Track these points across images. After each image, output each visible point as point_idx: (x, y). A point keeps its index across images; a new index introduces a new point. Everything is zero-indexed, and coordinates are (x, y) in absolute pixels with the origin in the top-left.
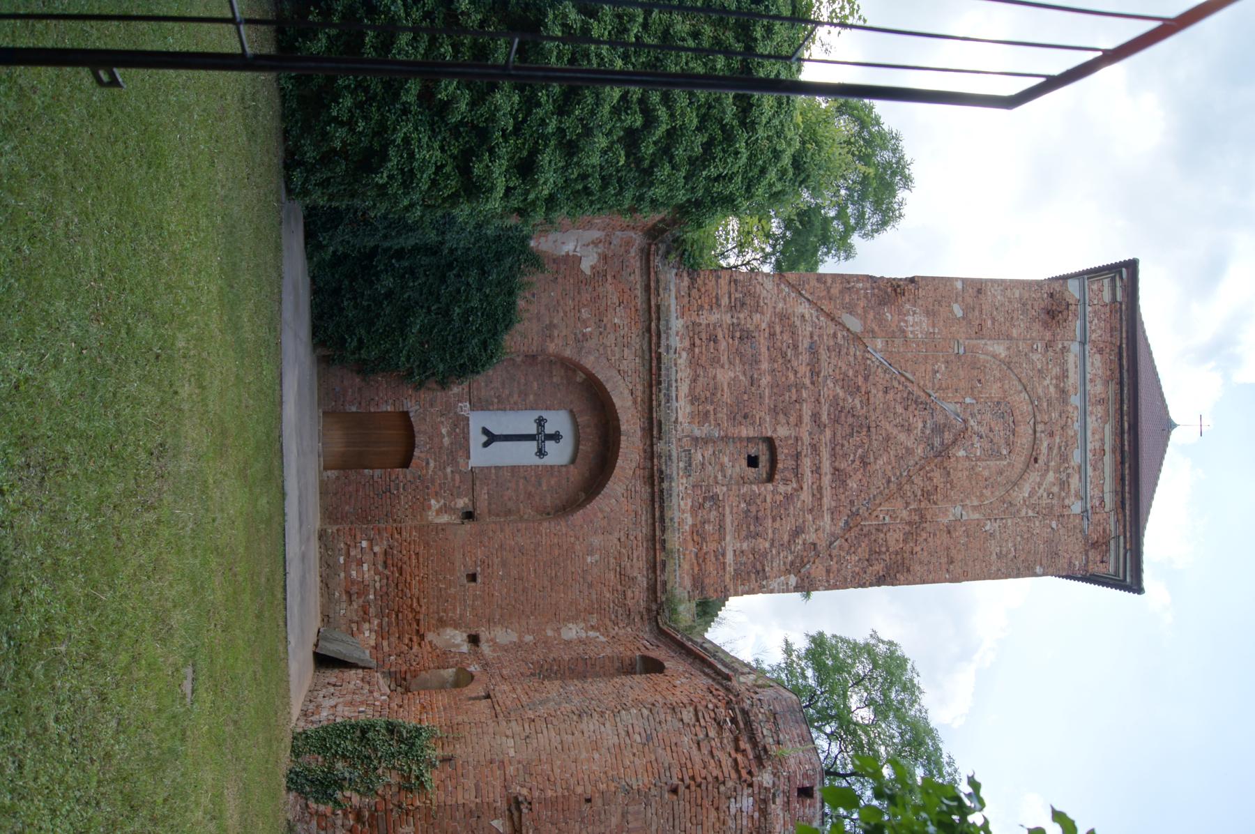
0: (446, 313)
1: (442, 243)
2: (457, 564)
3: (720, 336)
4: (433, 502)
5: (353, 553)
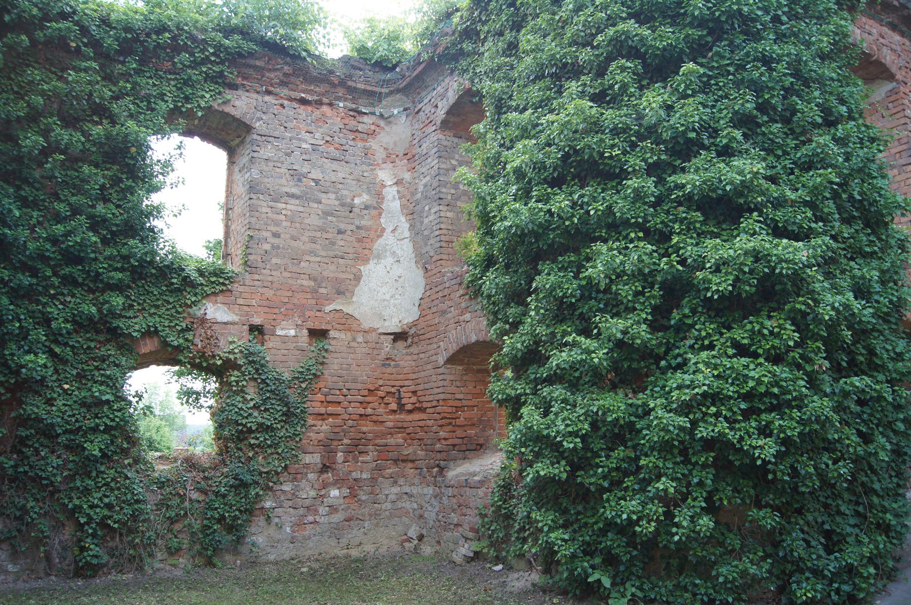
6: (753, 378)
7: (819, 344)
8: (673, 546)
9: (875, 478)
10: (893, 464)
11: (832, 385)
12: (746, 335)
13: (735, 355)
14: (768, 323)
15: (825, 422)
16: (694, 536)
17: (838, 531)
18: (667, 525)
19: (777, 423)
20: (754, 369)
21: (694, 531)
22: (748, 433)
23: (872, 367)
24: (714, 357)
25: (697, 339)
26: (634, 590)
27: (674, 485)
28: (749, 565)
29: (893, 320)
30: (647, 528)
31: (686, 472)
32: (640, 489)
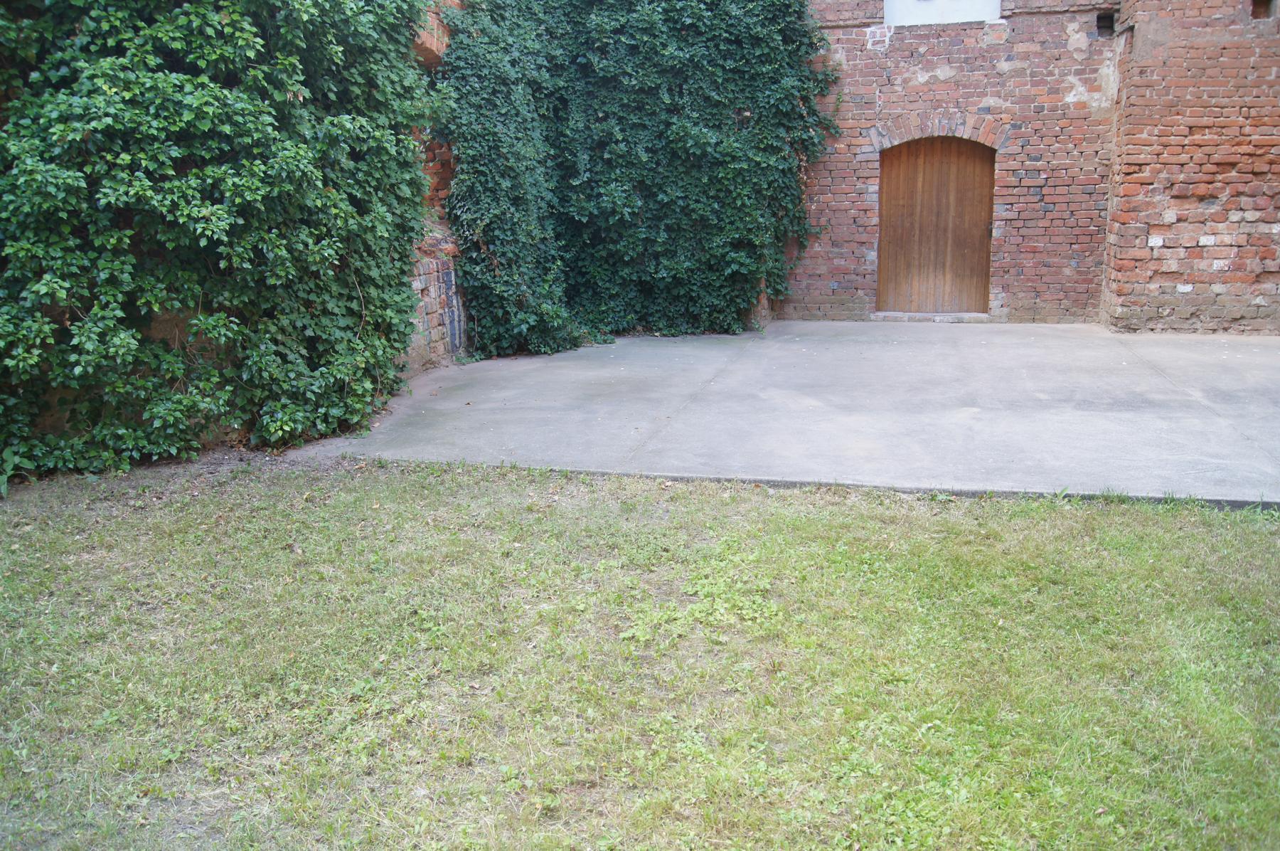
0: (678, 74)
1: (535, 86)
2: (1226, 39)
4: (1070, 98)
5: (1173, 266)
6: (189, 107)
7: (294, 60)
8: (74, 384)
9: (373, 263)
10: (396, 244)
11: (314, 127)
12: (178, 35)
13: (160, 68)
14: (215, 18)
15: (302, 182)
16: (108, 363)
17: (324, 337)
18: (63, 352)
19: (230, 182)
20: (191, 93)
21: (106, 357)
22: (184, 196)
23: (374, 105)
24: (124, 68)
25: (94, 35)
26: (17, 459)
27: (67, 285)
28: (199, 398)
29: (403, 40)
30: (25, 359)
31: (87, 263)
32: (10, 296)
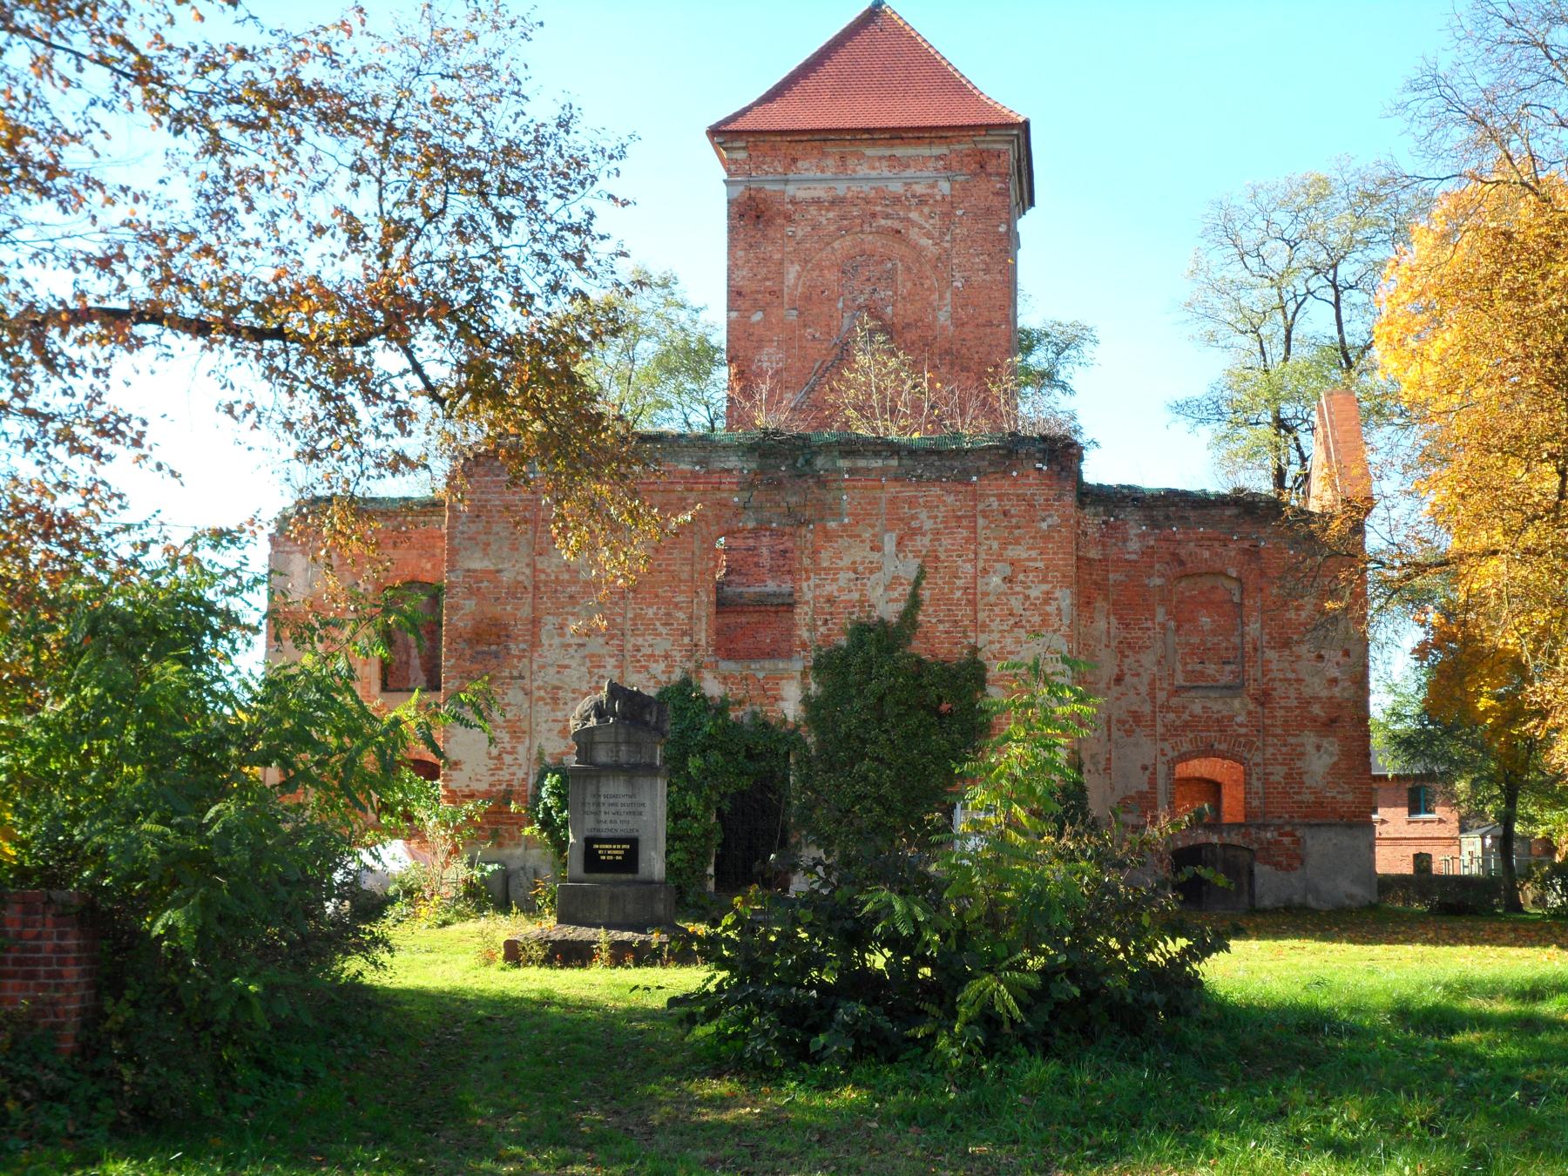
3: (782, 547)
